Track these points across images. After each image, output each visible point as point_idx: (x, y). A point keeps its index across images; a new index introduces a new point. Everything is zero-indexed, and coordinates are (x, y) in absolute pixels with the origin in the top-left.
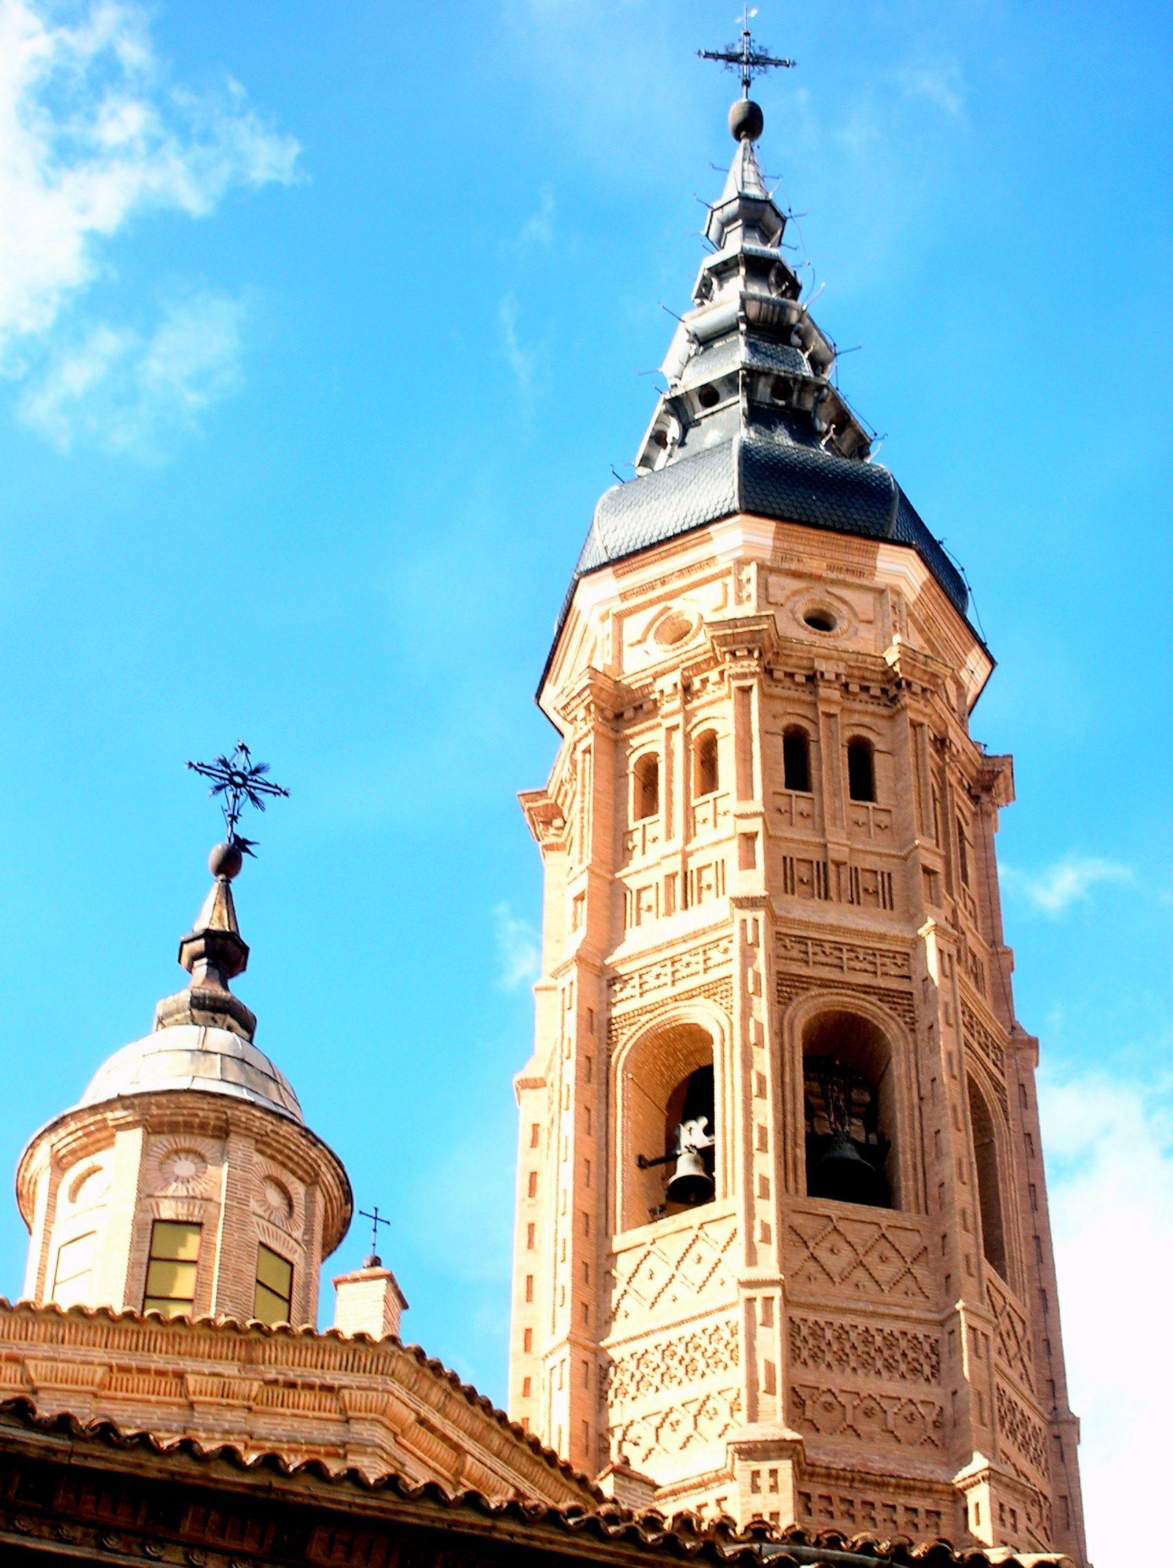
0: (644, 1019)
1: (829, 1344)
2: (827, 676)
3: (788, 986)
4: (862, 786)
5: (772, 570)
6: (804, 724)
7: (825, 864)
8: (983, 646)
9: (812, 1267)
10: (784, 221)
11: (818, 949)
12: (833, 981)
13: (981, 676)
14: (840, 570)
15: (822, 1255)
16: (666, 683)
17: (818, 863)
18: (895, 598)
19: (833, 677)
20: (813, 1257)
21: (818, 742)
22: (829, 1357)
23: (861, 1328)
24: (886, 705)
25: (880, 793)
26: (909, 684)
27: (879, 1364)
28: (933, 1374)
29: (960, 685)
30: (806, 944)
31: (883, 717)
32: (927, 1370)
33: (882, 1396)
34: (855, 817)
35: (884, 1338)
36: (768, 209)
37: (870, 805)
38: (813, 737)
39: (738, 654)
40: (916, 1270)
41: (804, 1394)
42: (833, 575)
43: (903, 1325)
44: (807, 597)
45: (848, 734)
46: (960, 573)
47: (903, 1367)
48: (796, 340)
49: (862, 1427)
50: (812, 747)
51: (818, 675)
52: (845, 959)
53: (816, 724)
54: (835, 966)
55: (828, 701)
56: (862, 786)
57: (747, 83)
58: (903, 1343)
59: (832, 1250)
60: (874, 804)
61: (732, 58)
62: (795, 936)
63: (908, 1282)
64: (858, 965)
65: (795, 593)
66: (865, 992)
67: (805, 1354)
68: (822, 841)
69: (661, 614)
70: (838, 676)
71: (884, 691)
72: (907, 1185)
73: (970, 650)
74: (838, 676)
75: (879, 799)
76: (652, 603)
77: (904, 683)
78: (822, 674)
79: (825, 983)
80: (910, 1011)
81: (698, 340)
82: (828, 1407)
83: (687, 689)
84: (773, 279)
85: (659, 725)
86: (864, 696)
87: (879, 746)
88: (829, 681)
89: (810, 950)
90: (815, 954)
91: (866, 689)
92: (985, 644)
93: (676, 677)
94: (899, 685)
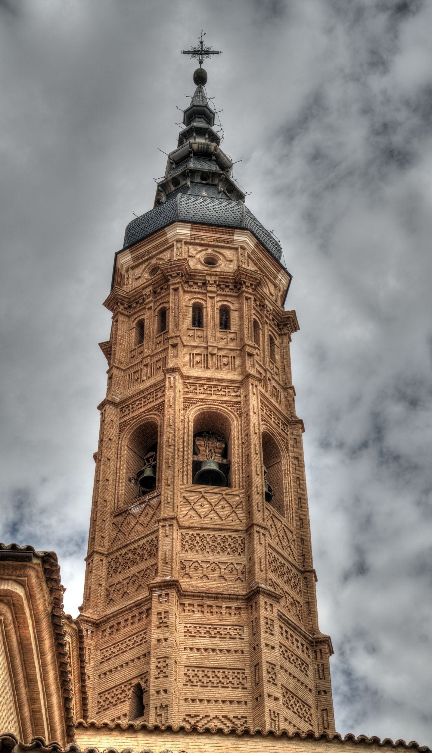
0: (132, 422)
1: (198, 543)
2: (211, 282)
3: (188, 403)
4: (225, 324)
5: (191, 244)
6: (201, 301)
7: (207, 355)
8: (285, 269)
9: (192, 513)
10: (214, 114)
11: (202, 388)
12: (207, 399)
13: (284, 282)
14: (219, 241)
15: (196, 507)
16: (147, 291)
17: (204, 355)
18: (242, 251)
19: (213, 282)
20: (193, 508)
21: (206, 308)
22: (197, 548)
23: (212, 535)
24: (236, 292)
25: (232, 326)
26: (245, 283)
27: (219, 549)
28: (242, 552)
29: (276, 286)
30: (197, 386)
31: (234, 296)
32: (239, 550)
33: (219, 562)
34: (221, 336)
35: (222, 539)
36: (206, 109)
37: (228, 331)
38: (205, 306)
39: (173, 275)
40: (237, 510)
41: (187, 564)
42: (217, 244)
43: (230, 533)
44: (205, 252)
45: (220, 304)
46: (278, 242)
47: (229, 550)
48: (214, 158)
49: (211, 576)
50: (205, 310)
51: (207, 282)
52: (213, 391)
53: (206, 301)
54: (209, 394)
55: (211, 292)
56: (225, 324)
57: (201, 62)
58: (229, 540)
59: (201, 505)
60: (230, 330)
61: (195, 53)
62: (192, 383)
63: (233, 516)
64: (217, 393)
65: (200, 251)
66: (221, 403)
67: (187, 547)
68: (206, 345)
69: (148, 265)
70: (215, 282)
71: (235, 287)
72: (236, 477)
73: (279, 272)
74: (215, 282)
75: (232, 329)
76: (145, 261)
77: (242, 282)
78: (209, 282)
79: (202, 400)
80: (240, 409)
81: (175, 162)
82: (196, 569)
83: (155, 292)
84: (207, 136)
85: (145, 308)
86: (227, 289)
87: (233, 308)
88: (212, 284)
89: (198, 388)
90: (200, 389)
91: (227, 286)
92: (286, 268)
93: (151, 288)
94: (241, 284)
